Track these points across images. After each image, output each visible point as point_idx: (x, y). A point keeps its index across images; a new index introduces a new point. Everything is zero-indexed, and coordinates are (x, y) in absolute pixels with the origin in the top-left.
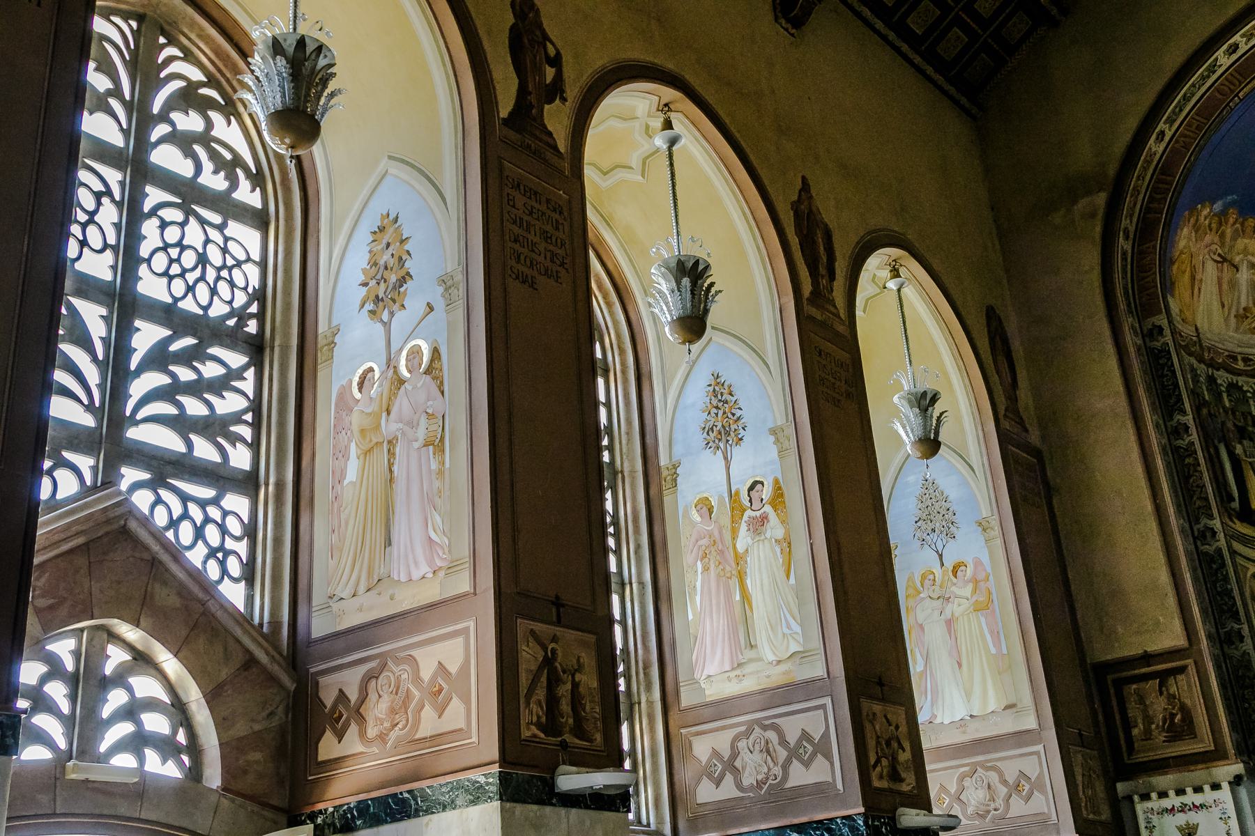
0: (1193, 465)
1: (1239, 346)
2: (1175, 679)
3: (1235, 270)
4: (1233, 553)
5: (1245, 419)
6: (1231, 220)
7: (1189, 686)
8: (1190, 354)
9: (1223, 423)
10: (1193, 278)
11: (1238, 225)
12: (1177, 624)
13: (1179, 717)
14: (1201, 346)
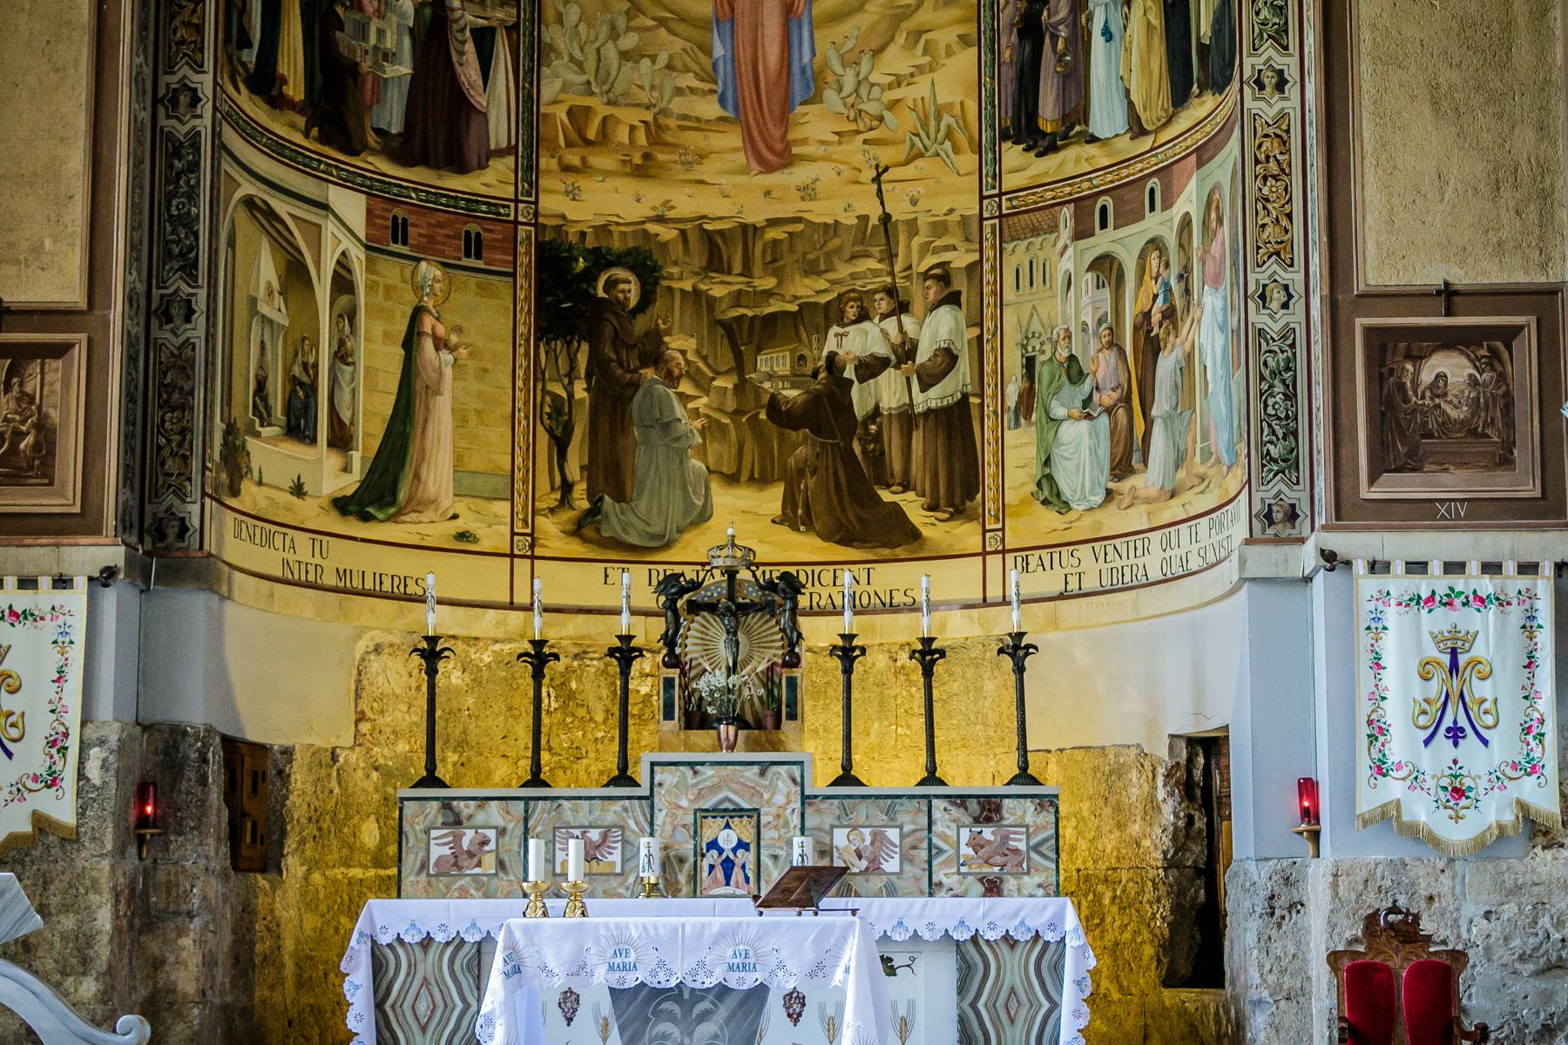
4: (220, 147)
7: (66, 382)
12: (74, 261)
13: (30, 439)
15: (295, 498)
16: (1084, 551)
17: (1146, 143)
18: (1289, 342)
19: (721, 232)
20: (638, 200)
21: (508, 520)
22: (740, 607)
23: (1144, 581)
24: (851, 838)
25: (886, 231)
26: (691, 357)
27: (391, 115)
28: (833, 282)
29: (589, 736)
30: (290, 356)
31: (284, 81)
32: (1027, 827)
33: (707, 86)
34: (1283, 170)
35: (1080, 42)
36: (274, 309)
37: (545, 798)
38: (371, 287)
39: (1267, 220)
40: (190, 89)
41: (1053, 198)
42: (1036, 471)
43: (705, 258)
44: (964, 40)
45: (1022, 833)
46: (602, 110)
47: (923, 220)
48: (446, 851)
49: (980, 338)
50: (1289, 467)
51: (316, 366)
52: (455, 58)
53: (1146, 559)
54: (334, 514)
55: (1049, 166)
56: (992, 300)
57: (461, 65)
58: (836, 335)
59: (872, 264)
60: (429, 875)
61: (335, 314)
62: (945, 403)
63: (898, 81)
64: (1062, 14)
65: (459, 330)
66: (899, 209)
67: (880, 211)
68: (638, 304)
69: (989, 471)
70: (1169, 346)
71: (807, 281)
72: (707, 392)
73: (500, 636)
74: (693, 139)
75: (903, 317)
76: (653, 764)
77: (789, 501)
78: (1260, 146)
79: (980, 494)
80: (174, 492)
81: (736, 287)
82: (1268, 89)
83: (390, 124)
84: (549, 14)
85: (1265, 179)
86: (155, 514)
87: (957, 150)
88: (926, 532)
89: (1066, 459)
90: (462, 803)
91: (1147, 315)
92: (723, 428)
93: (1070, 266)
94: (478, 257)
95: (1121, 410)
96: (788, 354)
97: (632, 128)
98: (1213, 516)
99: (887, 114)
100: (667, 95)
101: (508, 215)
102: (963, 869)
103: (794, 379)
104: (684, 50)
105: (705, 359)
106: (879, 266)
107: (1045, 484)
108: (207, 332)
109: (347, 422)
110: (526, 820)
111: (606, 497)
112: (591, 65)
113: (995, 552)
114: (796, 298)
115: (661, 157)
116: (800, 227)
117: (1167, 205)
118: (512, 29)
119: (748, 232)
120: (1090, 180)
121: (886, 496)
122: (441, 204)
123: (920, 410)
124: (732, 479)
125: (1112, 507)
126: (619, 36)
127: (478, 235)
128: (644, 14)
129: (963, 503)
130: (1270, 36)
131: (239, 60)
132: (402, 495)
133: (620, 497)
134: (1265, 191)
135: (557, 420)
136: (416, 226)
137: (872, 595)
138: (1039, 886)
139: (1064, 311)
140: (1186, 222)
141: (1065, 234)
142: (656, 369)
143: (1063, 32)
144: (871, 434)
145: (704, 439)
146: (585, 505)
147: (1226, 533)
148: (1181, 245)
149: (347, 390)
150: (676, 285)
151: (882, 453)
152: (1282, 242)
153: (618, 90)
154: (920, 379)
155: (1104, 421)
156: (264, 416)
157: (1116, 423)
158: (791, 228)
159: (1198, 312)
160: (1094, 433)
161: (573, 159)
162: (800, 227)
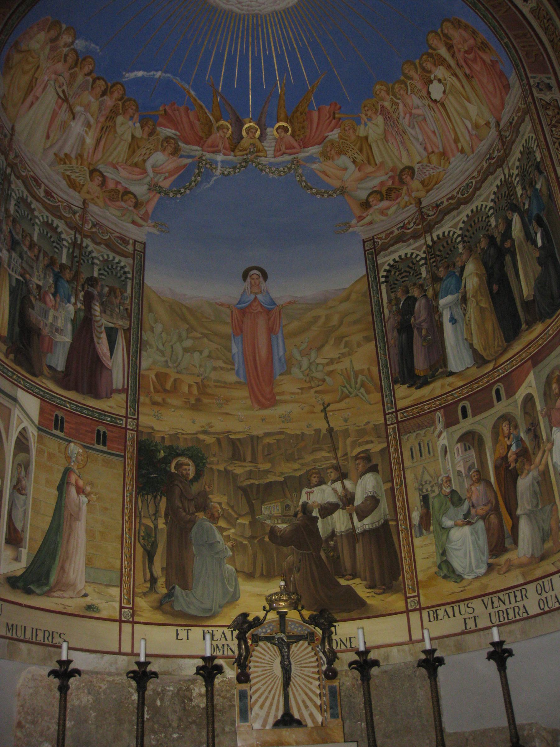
1: (47, 178)
3: (72, 117)
5: (24, 237)
6: (86, 70)
11: (90, 78)
16: (477, 604)
17: (491, 366)
19: (239, 440)
21: (118, 599)
23: (525, 615)
25: (331, 436)
28: (303, 465)
33: (229, 367)
38: (40, 452)
41: (429, 409)
42: (437, 559)
44: (367, 339)
46: (174, 376)
47: (351, 428)
52: (95, 340)
55: (425, 392)
56: (397, 467)
57: (99, 343)
58: (307, 493)
59: (325, 454)
62: (374, 526)
63: (332, 361)
64: (422, 318)
65: (91, 484)
66: (337, 424)
67: (327, 426)
68: (194, 477)
69: (406, 563)
70: (526, 472)
71: (288, 465)
72: (234, 526)
73: (113, 670)
75: (344, 481)
79: (401, 577)
81: (248, 469)
83: (57, 365)
88: (369, 601)
89: (456, 550)
91: (505, 458)
92: (244, 547)
93: (446, 442)
94: (104, 444)
95: (492, 516)
96: (279, 504)
97: (190, 386)
99: (328, 379)
101: (122, 424)
103: (284, 518)
104: (217, 349)
105: (232, 507)
106: (328, 455)
107: (444, 567)
109: (19, 529)
111: (177, 587)
113: (415, 610)
114: (282, 473)
115: (206, 401)
116: (282, 437)
117: (511, 393)
118: (127, 331)
119: (254, 440)
120: (453, 395)
121: (343, 582)
122: (84, 413)
123: (360, 531)
124: (250, 576)
125: (494, 574)
126: (182, 341)
127: (104, 433)
128: (196, 331)
132: (53, 579)
133: (185, 586)
135: (147, 540)
137: (339, 641)
140: (529, 399)
141: (440, 427)
142: (205, 513)
143: (425, 325)
144: (330, 547)
145: (233, 553)
146: (165, 591)
148: (526, 413)
149: (21, 510)
150: (214, 467)
151: (338, 557)
154: (357, 514)
155: (481, 525)
158: (278, 437)
159: (549, 445)
160: (475, 533)
161: (158, 398)
162: (282, 437)
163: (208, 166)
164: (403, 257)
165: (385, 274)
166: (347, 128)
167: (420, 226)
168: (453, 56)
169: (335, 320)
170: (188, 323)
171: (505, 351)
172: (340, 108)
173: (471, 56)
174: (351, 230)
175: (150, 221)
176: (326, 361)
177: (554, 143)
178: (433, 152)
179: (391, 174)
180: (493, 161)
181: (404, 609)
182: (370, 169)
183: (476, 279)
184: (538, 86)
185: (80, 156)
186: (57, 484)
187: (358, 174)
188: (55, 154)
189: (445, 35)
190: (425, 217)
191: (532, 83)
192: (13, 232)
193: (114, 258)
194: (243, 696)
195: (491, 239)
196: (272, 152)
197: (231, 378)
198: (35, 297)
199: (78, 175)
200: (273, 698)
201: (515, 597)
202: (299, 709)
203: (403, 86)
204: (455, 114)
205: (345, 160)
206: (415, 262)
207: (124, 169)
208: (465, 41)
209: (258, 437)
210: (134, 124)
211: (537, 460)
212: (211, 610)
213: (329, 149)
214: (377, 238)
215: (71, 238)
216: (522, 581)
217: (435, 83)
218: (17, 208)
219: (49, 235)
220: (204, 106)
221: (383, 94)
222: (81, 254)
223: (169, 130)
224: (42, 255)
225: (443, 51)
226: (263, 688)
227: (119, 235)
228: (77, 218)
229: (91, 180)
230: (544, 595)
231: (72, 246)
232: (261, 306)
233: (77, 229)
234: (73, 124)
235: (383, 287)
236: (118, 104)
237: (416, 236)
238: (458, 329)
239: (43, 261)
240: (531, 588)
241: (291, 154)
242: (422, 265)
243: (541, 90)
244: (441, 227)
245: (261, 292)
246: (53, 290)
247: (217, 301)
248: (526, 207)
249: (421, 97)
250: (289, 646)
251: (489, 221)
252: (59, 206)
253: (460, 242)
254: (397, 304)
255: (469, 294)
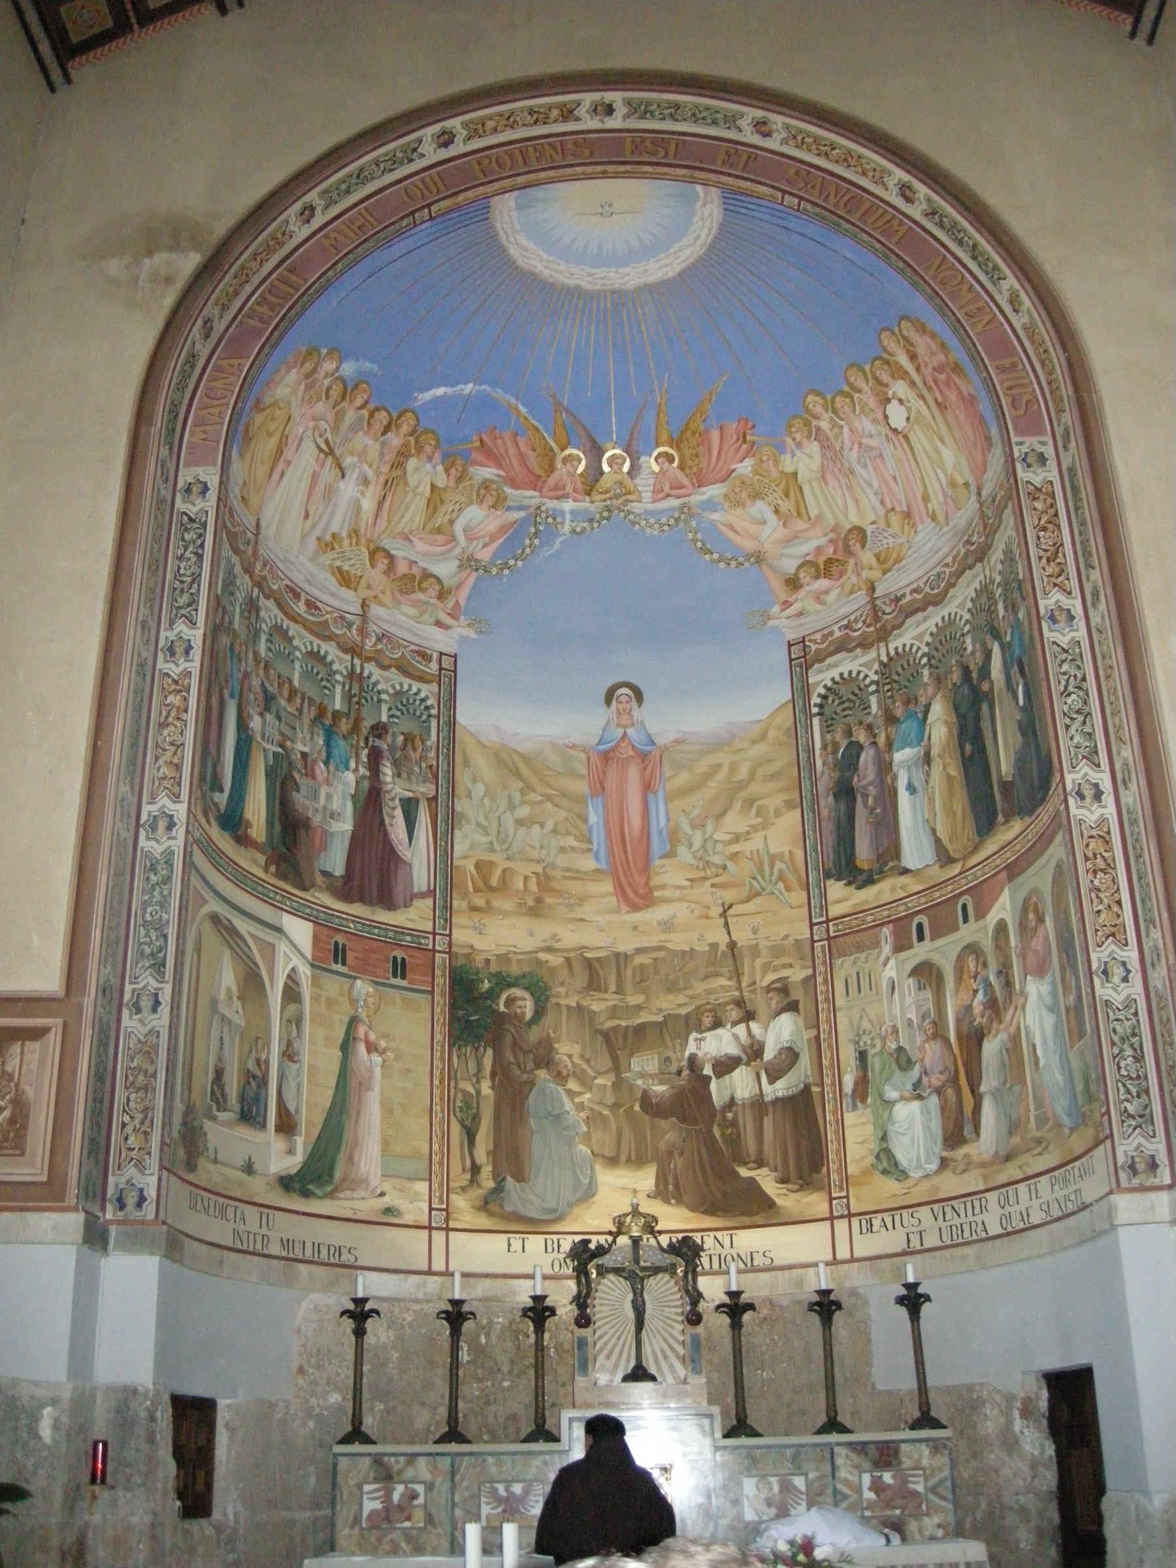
0: (178, 708)
2: (23, 1046)
6: (359, 401)
7: (42, 1063)
8: (237, 551)
9: (246, 675)
10: (280, 451)
11: (365, 413)
14: (255, 551)
15: (245, 1176)
16: (924, 1213)
17: (956, 869)
18: (1133, 1011)
19: (598, 959)
20: (532, 935)
21: (427, 1197)
22: (644, 1269)
23: (984, 1235)
24: (760, 1486)
25: (733, 955)
26: (576, 1060)
27: (335, 860)
28: (691, 997)
29: (497, 1385)
30: (247, 1049)
31: (249, 825)
32: (924, 1469)
33: (584, 846)
34: (1109, 865)
35: (889, 798)
36: (234, 1012)
37: (471, 1454)
38: (315, 999)
39: (1100, 907)
40: (167, 815)
42: (874, 1146)
43: (586, 979)
44: (789, 805)
45: (918, 1476)
46: (503, 864)
47: (763, 945)
48: (377, 1505)
49: (817, 1038)
50: (1146, 1122)
51: (267, 1062)
52: (387, 821)
53: (985, 1216)
54: (280, 1190)
55: (868, 895)
56: (826, 1006)
58: (696, 1040)
59: (723, 981)
60: (361, 1528)
61: (286, 1016)
63: (737, 838)
65: (386, 1036)
66: (742, 936)
67: (727, 939)
69: (832, 1148)
70: (993, 1032)
71: (670, 997)
73: (421, 1296)
74: (575, 887)
76: (570, 1419)
77: (661, 1179)
78: (1087, 845)
79: (824, 1169)
80: (135, 1165)
82: (1088, 800)
84: (460, 789)
85: (1095, 872)
86: (117, 1185)
87: (788, 889)
88: (779, 1201)
90: (393, 1459)
91: (969, 1008)
92: (605, 1120)
93: (893, 974)
94: (403, 977)
97: (526, 878)
98: (1056, 1173)
99: (729, 864)
100: (553, 852)
102: (867, 1513)
103: (662, 1076)
105: (588, 1061)
106: (729, 983)
107: (883, 1157)
108: (171, 1022)
109: (293, 1111)
110: (453, 1474)
111: (509, 1178)
112: (493, 829)
113: (842, 1217)
115: (549, 900)
116: (662, 954)
117: (981, 914)
119: (621, 959)
120: (906, 904)
121: (744, 1172)
124: (613, 1161)
125: (948, 1174)
127: (403, 959)
128: (534, 791)
129: (811, 1175)
130: (1084, 757)
131: (212, 799)
132: (338, 1175)
133: (520, 1177)
134: (1096, 882)
136: (352, 950)
138: (939, 1526)
139: (890, 1010)
140: (1001, 927)
141: (887, 949)
143: (872, 790)
145: (589, 1128)
146: (491, 1184)
147: (1072, 1188)
148: (998, 947)
150: (563, 1002)
151: (739, 1136)
152: (1115, 925)
153: (514, 848)
154: (767, 1073)
155: (934, 1101)
156: (219, 1099)
157: (946, 1101)
158: (655, 955)
159: (1022, 1000)
160: (926, 1111)
161: (480, 901)
162: (662, 954)
163: (550, 520)
164: (846, 675)
165: (818, 701)
166: (765, 458)
167: (872, 629)
168: (918, 369)
169: (743, 773)
170: (522, 781)
171: (976, 849)
172: (753, 427)
173: (942, 377)
174: (771, 623)
175: (462, 618)
176: (727, 837)
177: (1040, 558)
178: (893, 509)
179: (831, 535)
180: (972, 548)
181: (828, 1215)
182: (801, 525)
183: (944, 730)
184: (1024, 460)
185: (356, 532)
186: (340, 1041)
187: (782, 532)
188: (318, 539)
189: (906, 339)
190: (880, 614)
191: (1016, 454)
192: (267, 685)
193: (410, 686)
194: (582, 1343)
195: (966, 671)
196: (650, 494)
197: (588, 863)
198: (299, 772)
199: (352, 562)
200: (624, 1345)
201: (973, 1207)
202: (656, 1361)
203: (848, 400)
204: (924, 457)
205: (761, 508)
206: (862, 686)
207: (420, 539)
208: (933, 354)
209: (626, 956)
210: (434, 467)
211: (1008, 1018)
212: (555, 1210)
213: (737, 490)
214: (810, 641)
215: (346, 668)
216: (982, 1187)
217: (895, 403)
218: (269, 645)
219: (315, 671)
220: (541, 428)
221: (819, 409)
222: (361, 689)
223: (489, 470)
224: (306, 703)
225: (903, 359)
226: (611, 1333)
227: (416, 648)
228: (354, 632)
229: (373, 566)
230: (1008, 1209)
231: (348, 681)
232: (633, 747)
233: (353, 650)
234: (341, 485)
235: (816, 721)
236: (409, 442)
237: (865, 644)
238: (917, 803)
239: (310, 713)
240: (992, 1196)
241: (679, 497)
242: (872, 693)
243: (1029, 466)
244: (900, 635)
245: (633, 724)
246: (324, 754)
247: (567, 742)
248: (1008, 638)
249: (874, 421)
250: (642, 1279)
251: (964, 642)
252: (326, 621)
253: (925, 665)
254: (835, 752)
255: (935, 752)
